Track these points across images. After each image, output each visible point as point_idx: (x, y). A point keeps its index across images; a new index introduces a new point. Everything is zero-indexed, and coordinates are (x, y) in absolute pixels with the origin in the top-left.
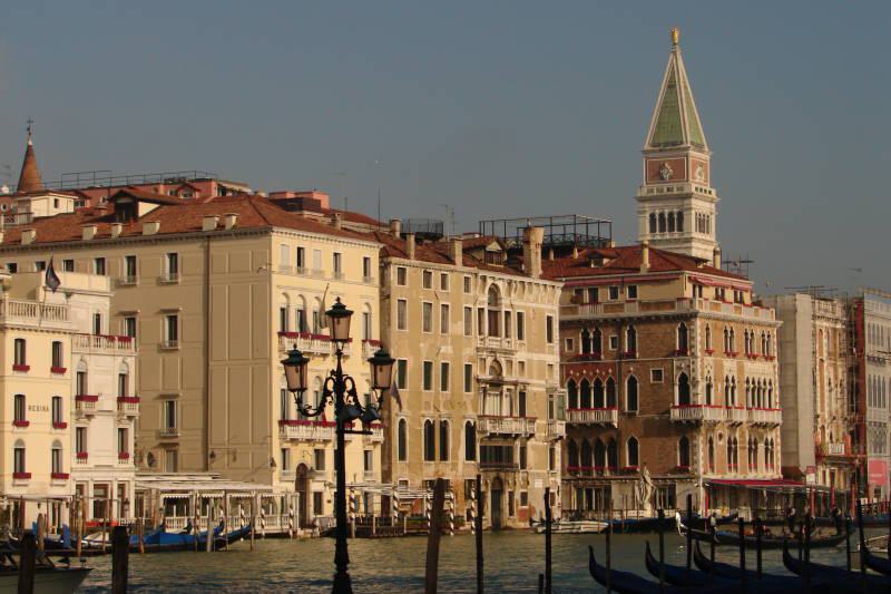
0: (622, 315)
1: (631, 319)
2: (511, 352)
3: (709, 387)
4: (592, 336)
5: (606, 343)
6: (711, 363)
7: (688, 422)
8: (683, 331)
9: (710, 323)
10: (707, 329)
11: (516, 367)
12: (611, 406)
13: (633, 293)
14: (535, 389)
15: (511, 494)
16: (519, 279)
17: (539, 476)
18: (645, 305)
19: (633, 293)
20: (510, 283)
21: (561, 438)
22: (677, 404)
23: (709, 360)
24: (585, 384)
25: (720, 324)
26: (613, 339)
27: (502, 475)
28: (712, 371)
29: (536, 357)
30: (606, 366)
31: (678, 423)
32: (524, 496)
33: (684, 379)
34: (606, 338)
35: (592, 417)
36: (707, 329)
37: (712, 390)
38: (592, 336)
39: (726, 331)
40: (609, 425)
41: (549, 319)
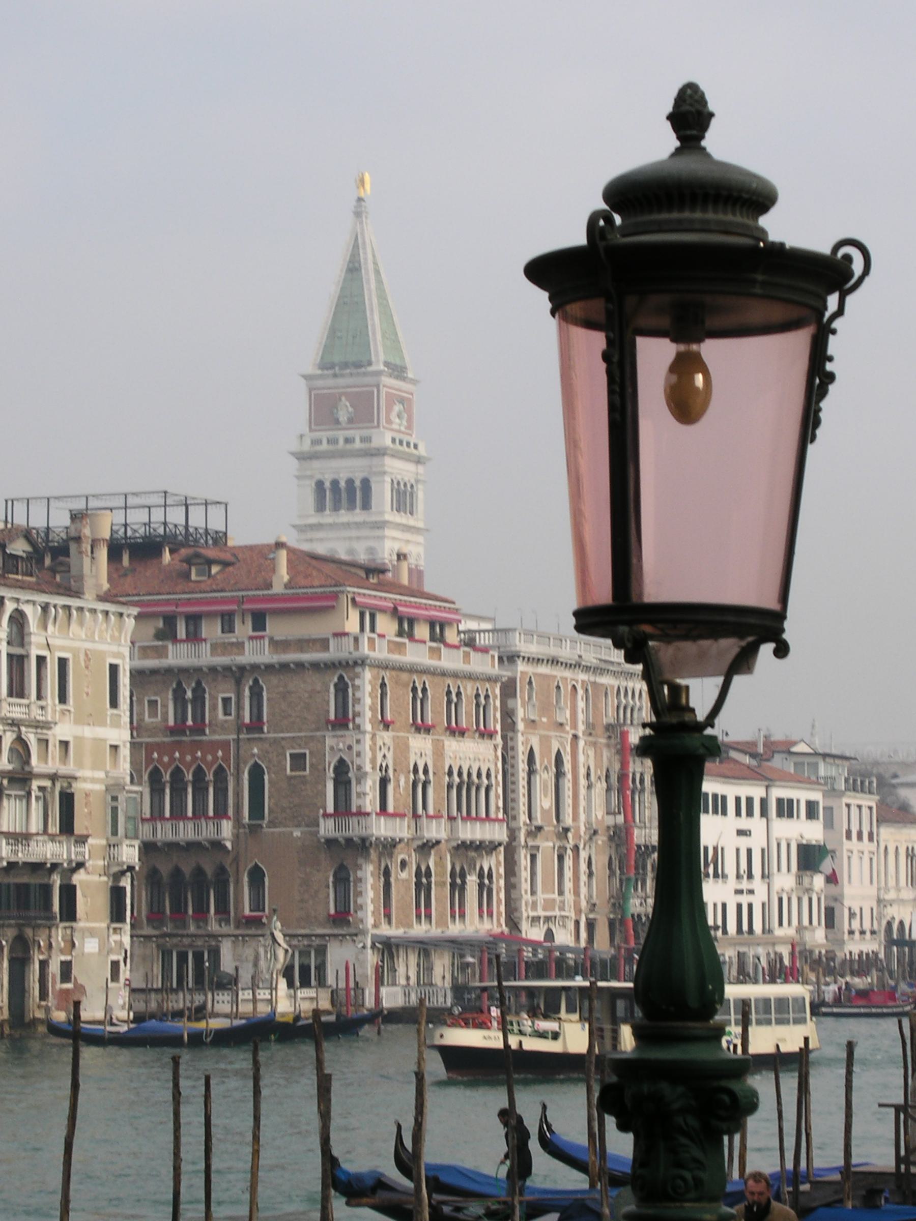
1: (255, 667)
2: (47, 725)
3: (384, 782)
4: (189, 694)
5: (214, 708)
6: (389, 742)
7: (349, 841)
8: (342, 689)
9: (387, 675)
10: (383, 685)
11: (54, 749)
12: (221, 813)
14: (88, 786)
15: (44, 964)
16: (61, 601)
17: (92, 933)
18: (278, 645)
20: (45, 608)
21: (131, 868)
22: (330, 809)
23: (386, 737)
24: (177, 774)
25: (405, 676)
26: (226, 701)
27: (29, 932)
28: (390, 756)
29: (88, 732)
30: (214, 746)
31: (331, 843)
32: (66, 970)
33: (342, 768)
34: (214, 698)
35: (186, 832)
36: (383, 685)
38: (189, 694)
39: (414, 689)
40: (217, 845)
41: (114, 669)
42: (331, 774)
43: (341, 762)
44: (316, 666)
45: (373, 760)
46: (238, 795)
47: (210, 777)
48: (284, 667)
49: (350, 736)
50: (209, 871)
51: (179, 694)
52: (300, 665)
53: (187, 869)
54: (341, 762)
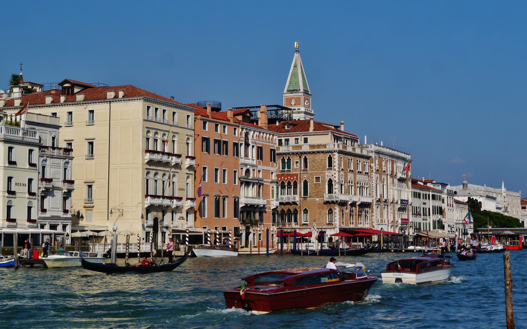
0: (301, 151)
1: (305, 153)
4: (286, 161)
5: (293, 164)
8: (330, 159)
13: (306, 141)
18: (312, 146)
19: (306, 141)
30: (293, 175)
33: (330, 181)
34: (293, 162)
37: (343, 187)
38: (286, 161)
40: (295, 203)
42: (327, 183)
43: (330, 179)
44: (323, 152)
45: (339, 179)
46: (300, 189)
47: (292, 184)
48: (314, 153)
49: (333, 172)
50: (292, 210)
51: (283, 160)
52: (318, 152)
53: (286, 210)
54: (330, 179)
